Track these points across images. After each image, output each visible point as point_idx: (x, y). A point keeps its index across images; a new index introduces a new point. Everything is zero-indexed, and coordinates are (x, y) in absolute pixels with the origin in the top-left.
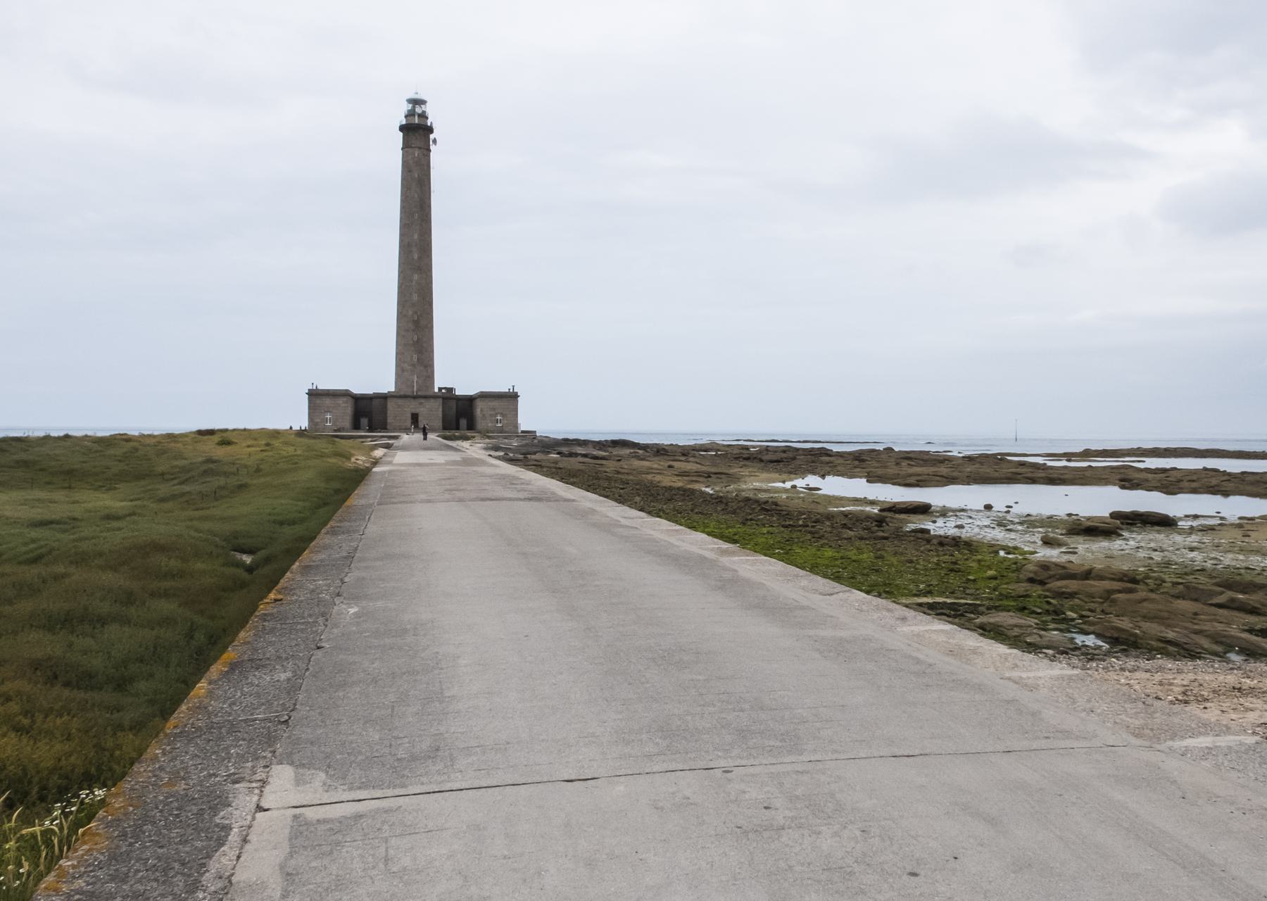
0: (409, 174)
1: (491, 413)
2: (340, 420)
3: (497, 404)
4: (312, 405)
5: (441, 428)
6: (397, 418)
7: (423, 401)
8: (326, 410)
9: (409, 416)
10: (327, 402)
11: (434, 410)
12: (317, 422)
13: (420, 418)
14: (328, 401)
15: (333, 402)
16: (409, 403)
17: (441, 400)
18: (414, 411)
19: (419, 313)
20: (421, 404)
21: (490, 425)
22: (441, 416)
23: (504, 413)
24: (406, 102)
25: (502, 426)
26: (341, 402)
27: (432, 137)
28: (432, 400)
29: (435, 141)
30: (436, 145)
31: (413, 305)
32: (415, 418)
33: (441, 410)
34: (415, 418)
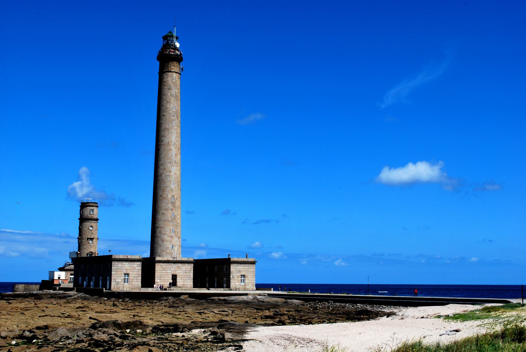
0: (169, 91)
1: (238, 274)
2: (135, 280)
3: (242, 268)
5: (193, 287)
6: (162, 278)
7: (180, 265)
8: (125, 272)
9: (171, 276)
10: (126, 265)
11: (187, 272)
12: (118, 282)
13: (178, 279)
14: (126, 265)
15: (130, 265)
18: (174, 273)
19: (176, 196)
20: (179, 267)
21: (237, 284)
22: (192, 276)
23: (246, 275)
24: (162, 40)
26: (136, 266)
28: (187, 265)
32: (174, 277)
33: (192, 272)
34: (174, 277)
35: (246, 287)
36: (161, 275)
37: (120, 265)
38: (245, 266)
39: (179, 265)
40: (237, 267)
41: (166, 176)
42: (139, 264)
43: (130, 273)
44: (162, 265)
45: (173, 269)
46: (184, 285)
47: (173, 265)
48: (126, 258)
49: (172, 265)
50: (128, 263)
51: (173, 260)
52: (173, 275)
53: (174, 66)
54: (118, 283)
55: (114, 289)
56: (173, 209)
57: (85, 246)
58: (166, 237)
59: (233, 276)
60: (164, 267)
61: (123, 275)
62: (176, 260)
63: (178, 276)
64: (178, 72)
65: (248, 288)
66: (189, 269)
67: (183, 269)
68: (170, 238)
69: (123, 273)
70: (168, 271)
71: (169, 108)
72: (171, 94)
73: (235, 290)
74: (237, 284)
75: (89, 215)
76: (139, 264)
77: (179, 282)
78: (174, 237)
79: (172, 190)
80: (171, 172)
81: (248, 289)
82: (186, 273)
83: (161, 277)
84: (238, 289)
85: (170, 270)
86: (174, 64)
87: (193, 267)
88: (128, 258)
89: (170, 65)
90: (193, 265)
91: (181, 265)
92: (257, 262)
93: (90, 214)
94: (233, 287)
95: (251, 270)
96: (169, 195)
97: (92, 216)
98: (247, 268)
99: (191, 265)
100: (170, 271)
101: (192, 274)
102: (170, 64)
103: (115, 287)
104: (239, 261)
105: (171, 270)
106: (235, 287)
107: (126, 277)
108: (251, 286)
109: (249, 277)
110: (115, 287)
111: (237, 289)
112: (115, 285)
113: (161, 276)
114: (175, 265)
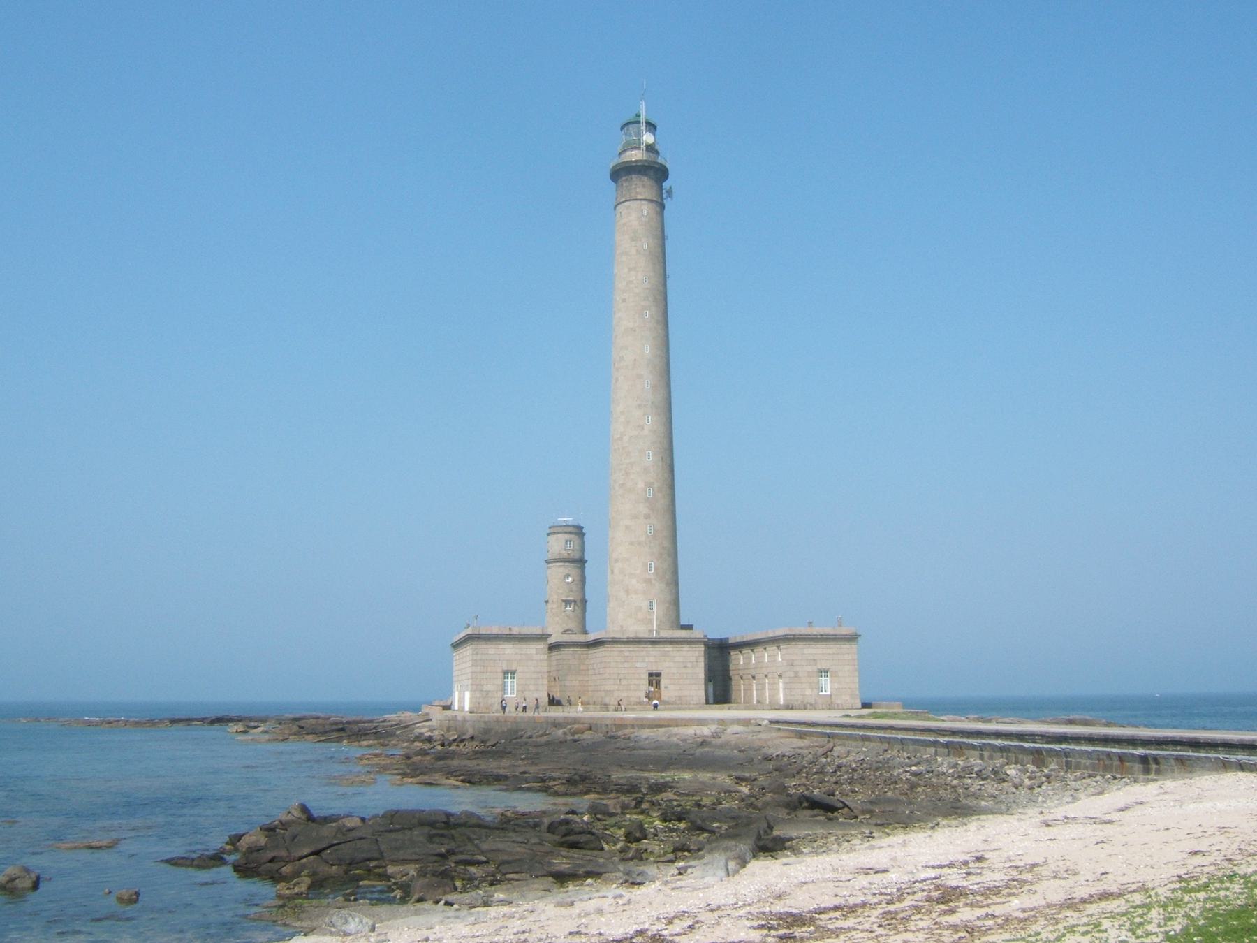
0: (633, 243)
1: (809, 668)
2: (532, 688)
3: (820, 651)
4: (479, 657)
6: (624, 682)
7: (669, 648)
10: (508, 651)
11: (689, 665)
12: (488, 692)
14: (508, 649)
15: (517, 651)
16: (644, 653)
17: (702, 648)
18: (654, 669)
25: (831, 696)
26: (534, 651)
27: (666, 185)
28: (686, 648)
29: (670, 193)
30: (672, 199)
31: (646, 470)
32: (654, 678)
33: (702, 665)
34: (654, 678)
35: (833, 700)
36: (619, 674)
37: (492, 651)
38: (828, 646)
39: (667, 649)
40: (806, 651)
41: (631, 437)
42: (542, 646)
43: (519, 670)
44: (623, 649)
45: (652, 659)
46: (680, 697)
47: (649, 648)
48: (508, 633)
49: (648, 649)
50: (511, 646)
51: (651, 637)
52: (651, 675)
53: (644, 186)
54: (487, 694)
55: (476, 707)
56: (649, 515)
57: (557, 616)
58: (634, 581)
59: (796, 673)
60: (627, 654)
61: (501, 675)
62: (658, 637)
63: (663, 675)
64: (654, 199)
65: (839, 702)
66: (694, 659)
67: (677, 659)
68: (644, 585)
69: (499, 670)
70: (638, 665)
71: (635, 282)
72: (637, 251)
73: (803, 708)
74: (808, 692)
75: (563, 552)
76: (542, 646)
77: (669, 690)
78: (653, 582)
79: (645, 469)
80: (643, 429)
81: (838, 705)
82: (685, 667)
83: (620, 680)
84: (811, 705)
85: (643, 662)
86: (643, 181)
87: (702, 653)
88: (512, 633)
89: (633, 186)
90: (703, 649)
91: (671, 649)
92: (860, 636)
93: (565, 550)
94: (797, 700)
95: (846, 657)
96: (640, 483)
97: (569, 554)
98: (834, 651)
99: (697, 649)
100: (644, 665)
101: (703, 670)
102: (635, 183)
103: (479, 703)
104: (810, 635)
105: (647, 660)
106: (802, 702)
107: (508, 678)
108: (848, 697)
109: (840, 674)
110: (482, 705)
111: (808, 706)
112: (481, 700)
113: (621, 677)
114: (657, 649)
